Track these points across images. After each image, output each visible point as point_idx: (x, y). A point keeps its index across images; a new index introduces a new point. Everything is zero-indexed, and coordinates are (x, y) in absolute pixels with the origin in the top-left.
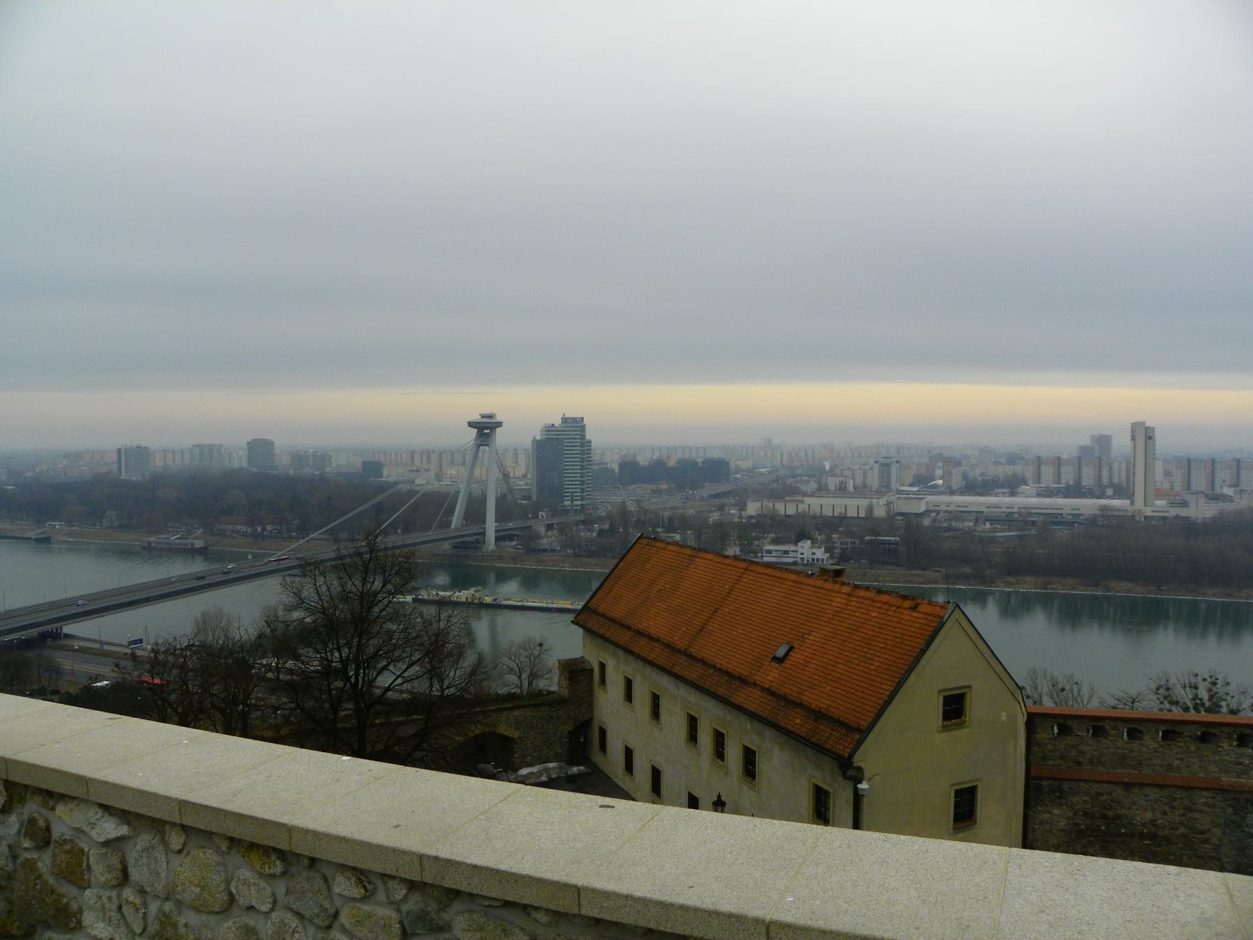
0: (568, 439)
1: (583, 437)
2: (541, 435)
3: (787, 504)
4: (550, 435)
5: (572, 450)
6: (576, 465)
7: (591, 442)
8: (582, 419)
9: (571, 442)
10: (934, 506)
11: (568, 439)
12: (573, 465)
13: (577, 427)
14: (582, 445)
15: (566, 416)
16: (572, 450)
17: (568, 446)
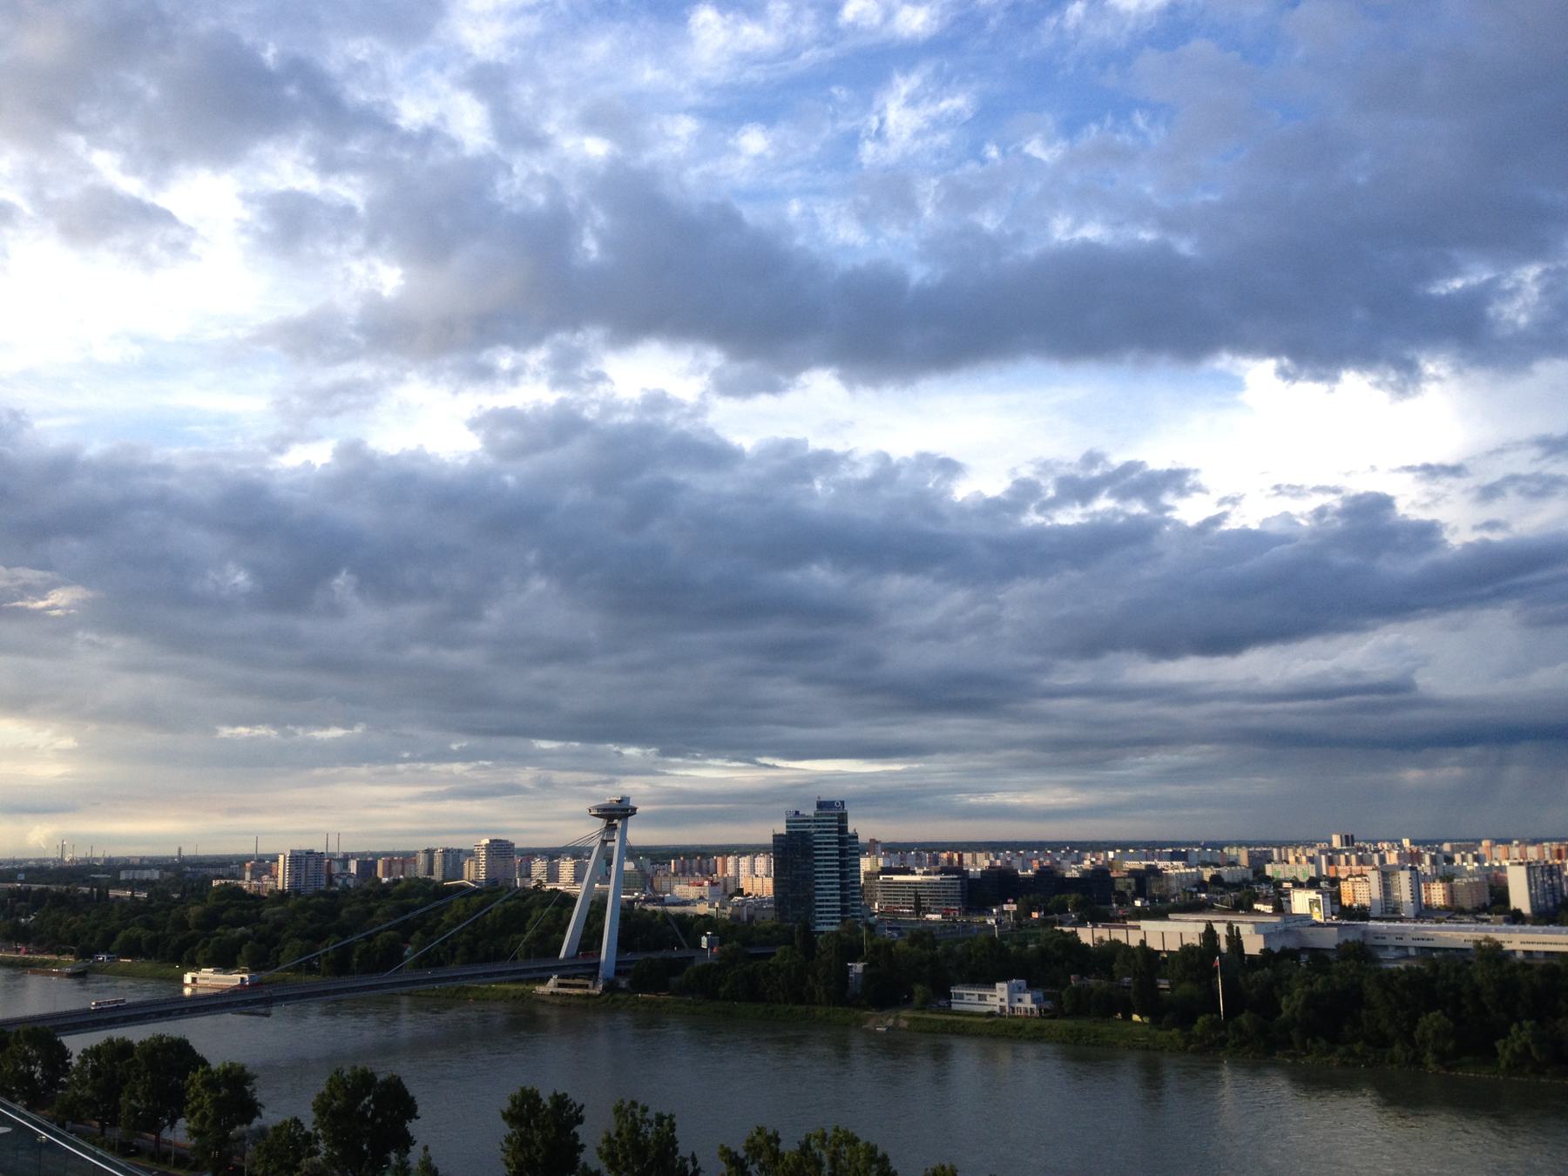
0: (820, 832)
1: (843, 830)
2: (787, 827)
3: (1129, 931)
4: (794, 827)
5: (826, 849)
6: (833, 872)
7: (857, 837)
8: (843, 803)
9: (823, 838)
10: (1377, 938)
11: (820, 832)
12: (827, 872)
13: (832, 815)
14: (842, 842)
15: (821, 800)
16: (826, 849)
17: (820, 843)
